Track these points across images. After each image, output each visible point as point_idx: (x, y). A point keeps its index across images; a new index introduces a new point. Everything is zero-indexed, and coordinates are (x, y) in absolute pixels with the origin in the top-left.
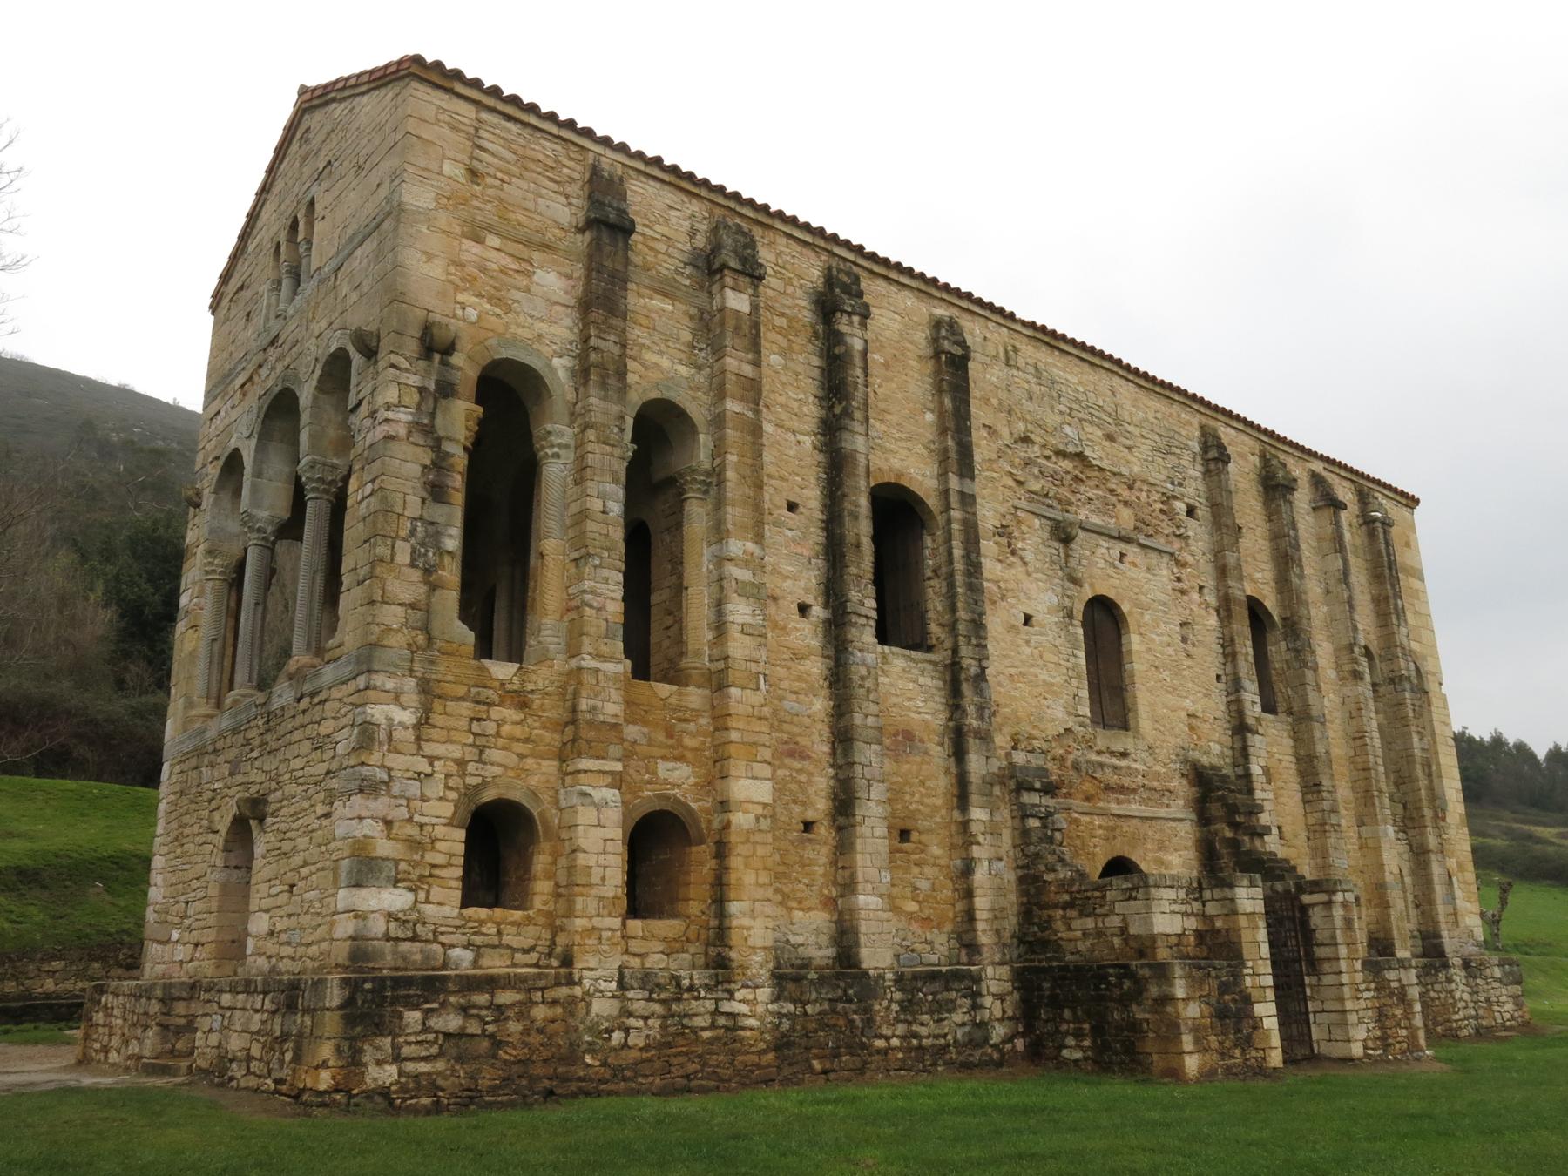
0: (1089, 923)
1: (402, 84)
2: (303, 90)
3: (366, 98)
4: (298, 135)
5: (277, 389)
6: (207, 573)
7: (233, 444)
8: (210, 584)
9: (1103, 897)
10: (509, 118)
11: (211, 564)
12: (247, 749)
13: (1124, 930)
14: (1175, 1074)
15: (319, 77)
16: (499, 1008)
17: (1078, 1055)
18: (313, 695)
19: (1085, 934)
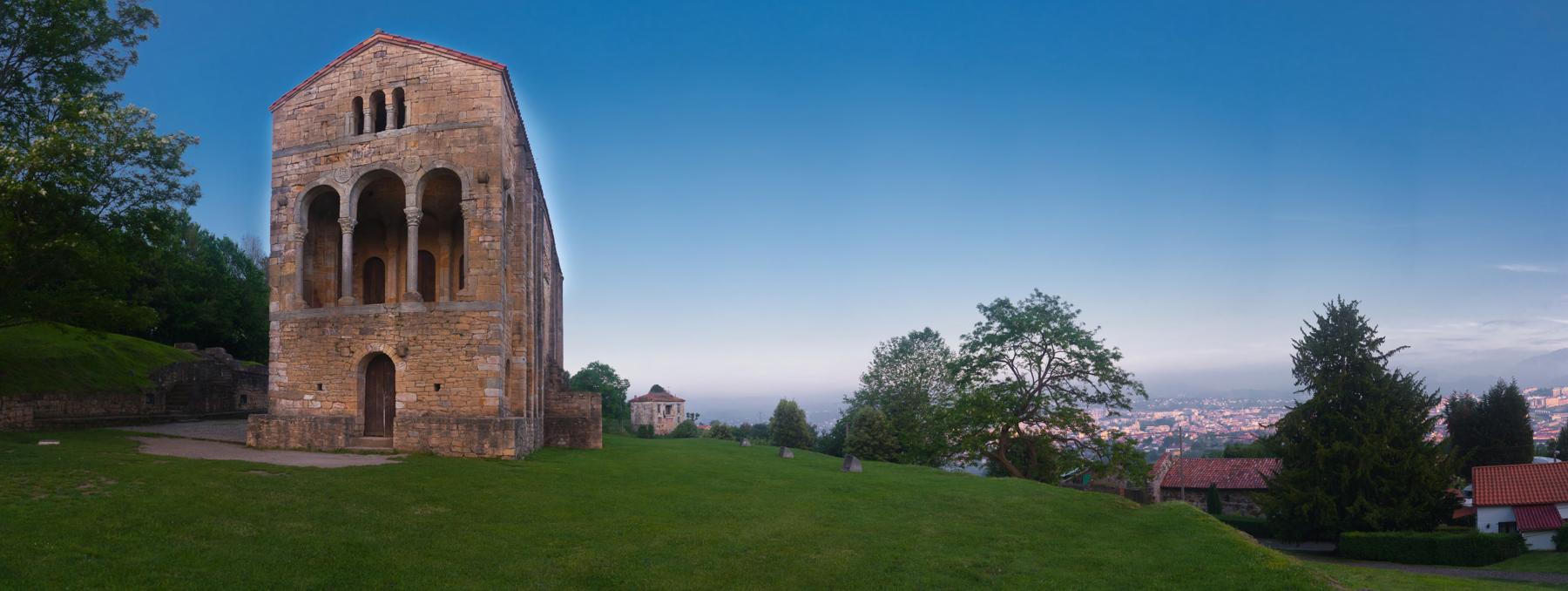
5: (377, 167)
7: (321, 181)
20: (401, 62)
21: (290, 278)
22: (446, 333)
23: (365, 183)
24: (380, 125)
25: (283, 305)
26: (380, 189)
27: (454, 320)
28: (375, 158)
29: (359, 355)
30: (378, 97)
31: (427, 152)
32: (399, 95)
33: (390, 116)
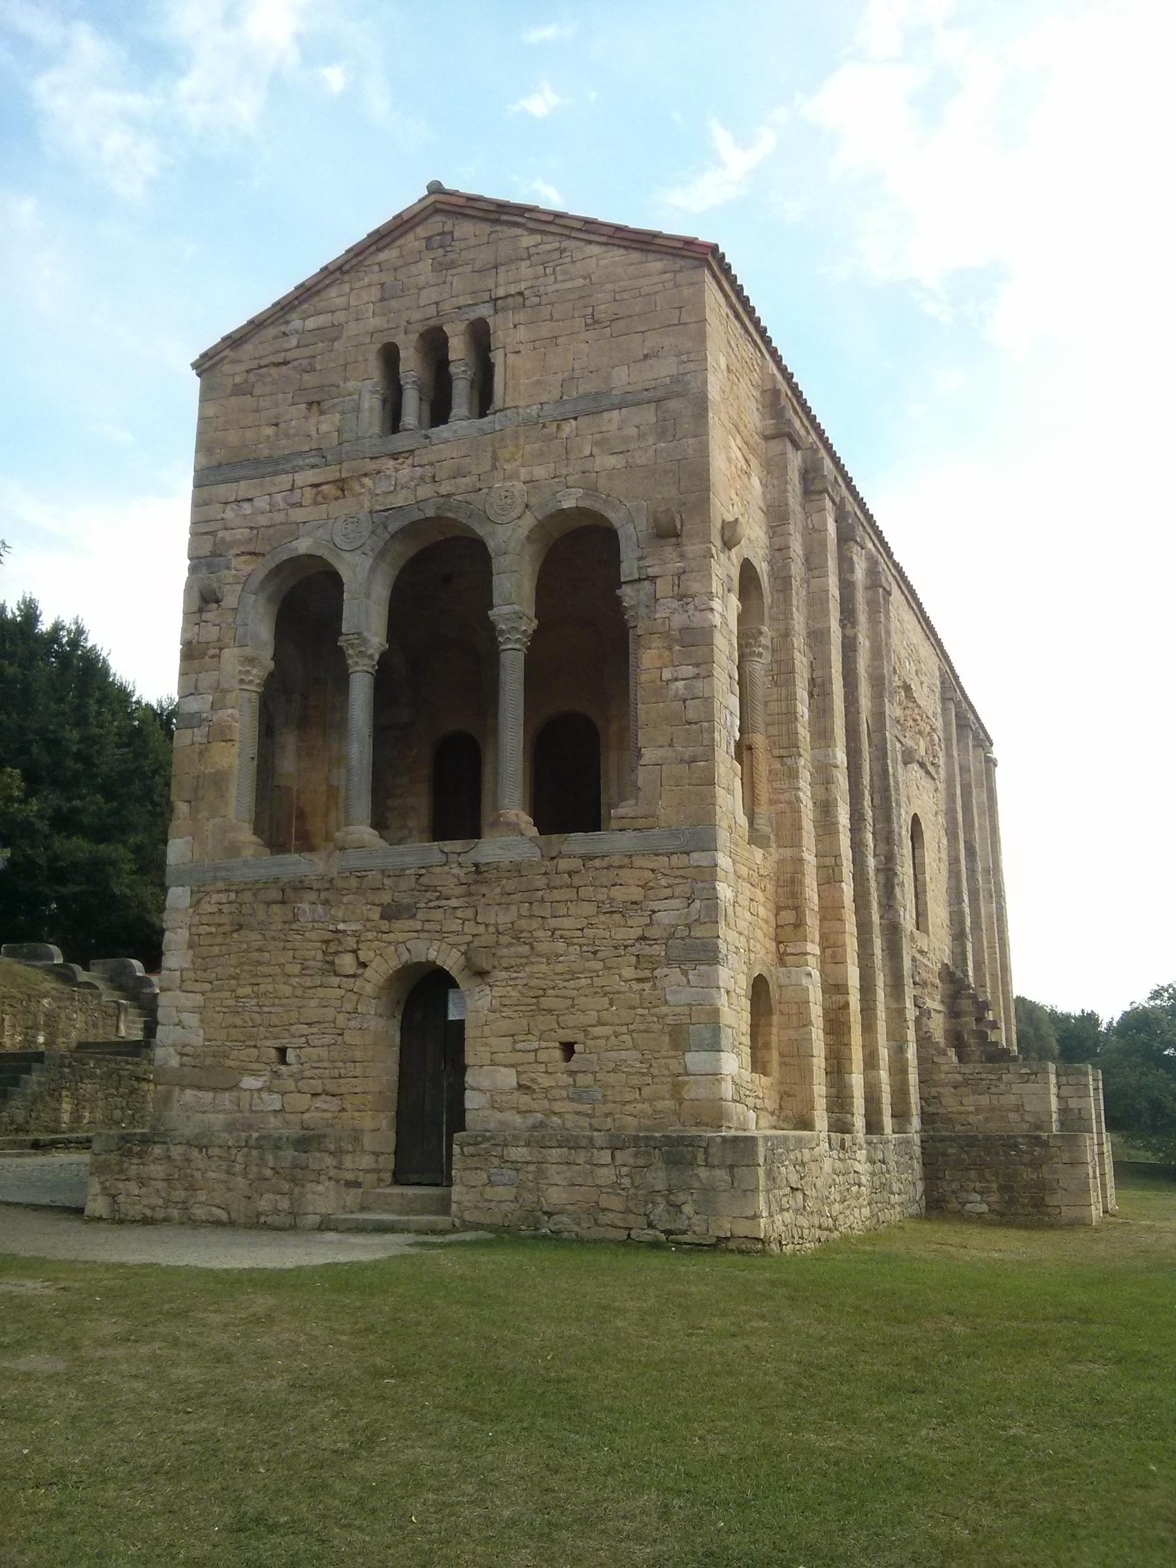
0: (984, 1100)
1: (682, 263)
2: (435, 188)
3: (595, 249)
4: (421, 231)
5: (430, 513)
6: (242, 681)
7: (303, 546)
8: (247, 694)
9: (1000, 1079)
10: (737, 316)
11: (248, 671)
12: (428, 895)
13: (1019, 1108)
14: (1081, 1223)
15: (470, 179)
16: (803, 1164)
17: (984, 1208)
18: (587, 858)
19: (978, 1111)
20: (484, 256)
21: (219, 780)
22: (589, 909)
23: (407, 550)
24: (439, 412)
25: (207, 837)
26: (440, 566)
27: (606, 877)
28: (424, 491)
29: (381, 968)
30: (434, 343)
31: (540, 472)
32: (481, 338)
33: (461, 390)
